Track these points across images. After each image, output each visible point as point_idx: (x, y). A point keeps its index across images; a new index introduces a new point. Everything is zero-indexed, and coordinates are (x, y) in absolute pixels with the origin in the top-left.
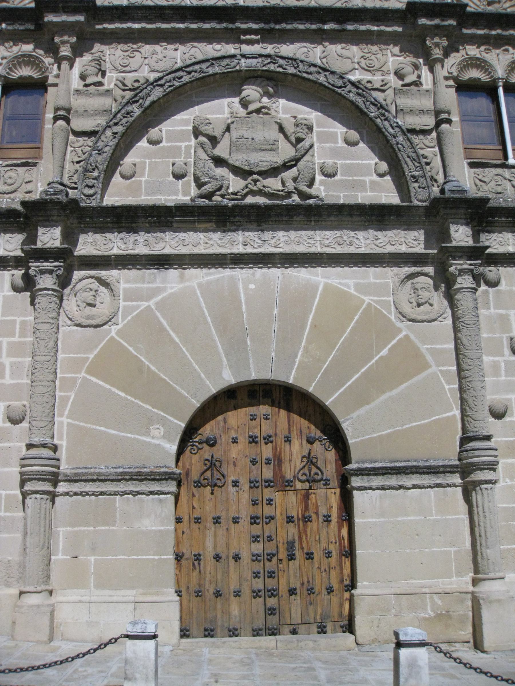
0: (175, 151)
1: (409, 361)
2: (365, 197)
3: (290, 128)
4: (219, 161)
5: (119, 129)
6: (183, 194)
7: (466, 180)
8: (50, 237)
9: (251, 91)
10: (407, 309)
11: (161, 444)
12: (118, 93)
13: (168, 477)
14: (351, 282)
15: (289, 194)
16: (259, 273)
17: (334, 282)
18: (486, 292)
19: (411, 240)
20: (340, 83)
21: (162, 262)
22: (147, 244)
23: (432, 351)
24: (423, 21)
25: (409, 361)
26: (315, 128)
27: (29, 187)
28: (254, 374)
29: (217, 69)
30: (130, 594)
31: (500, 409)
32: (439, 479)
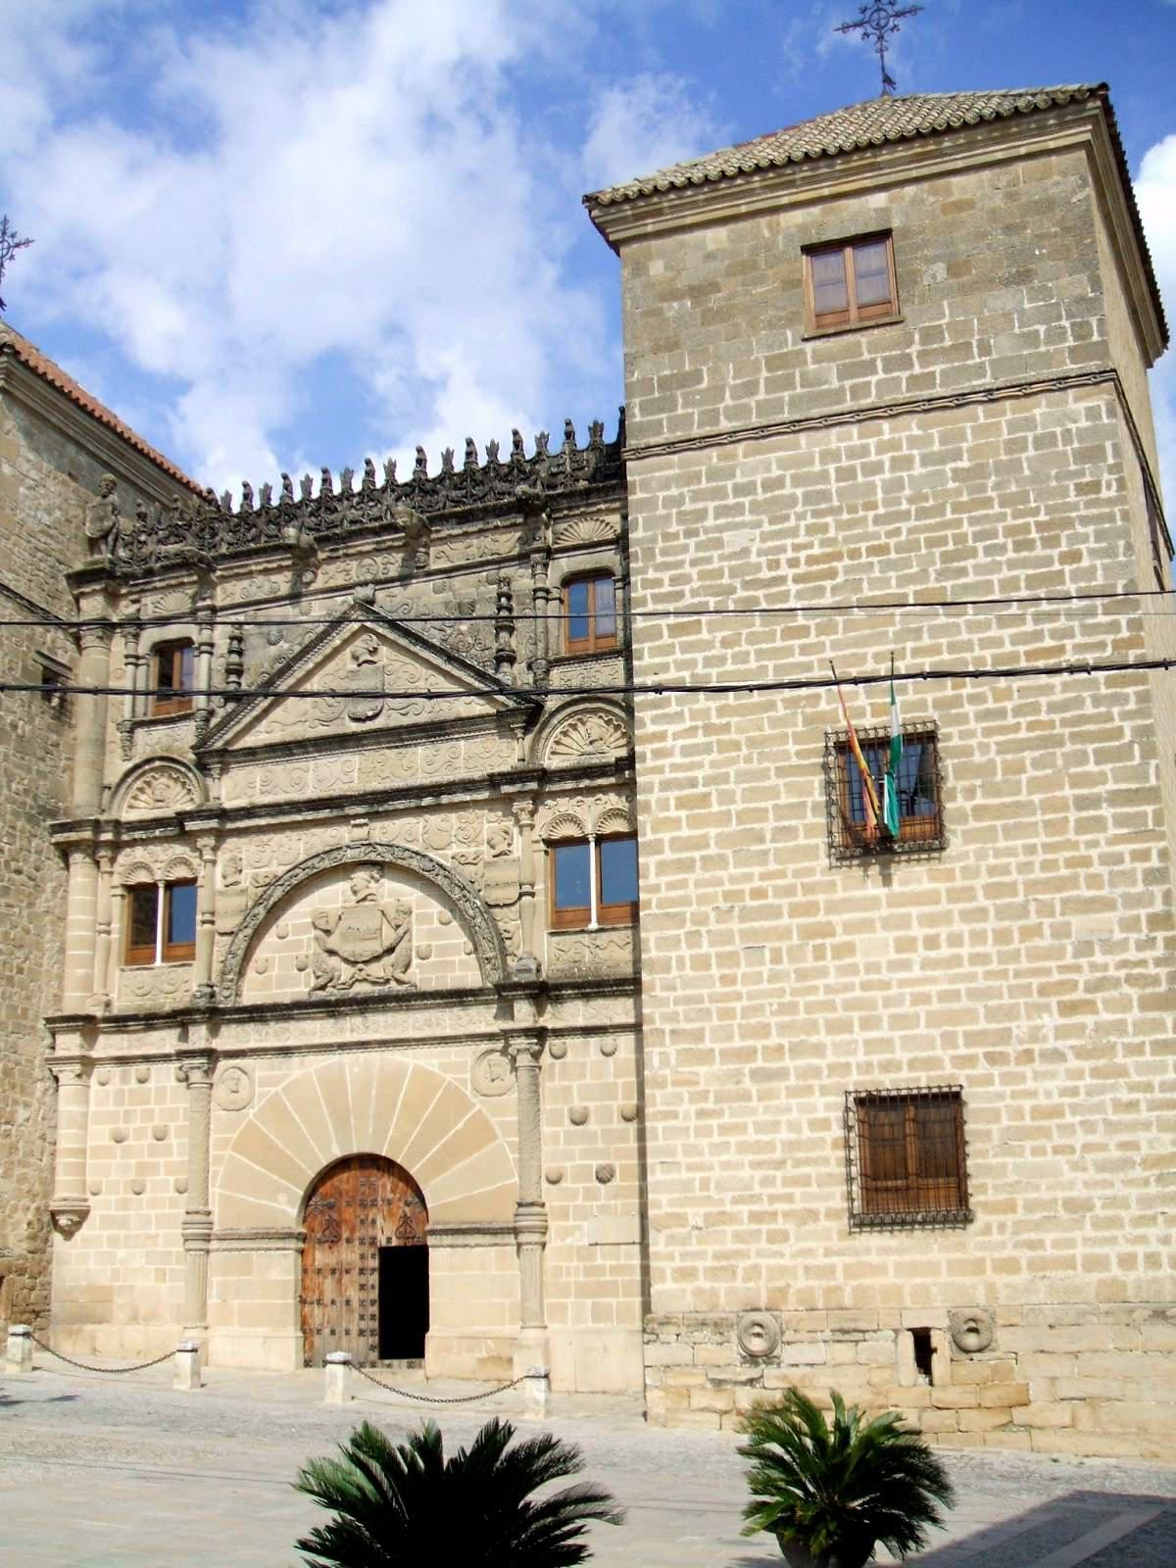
0: (299, 944)
1: (480, 1132)
2: (451, 981)
3: (391, 914)
4: (331, 953)
5: (249, 931)
6: (300, 988)
7: (542, 950)
8: (199, 1036)
9: (361, 876)
10: (485, 1085)
11: (287, 1210)
12: (252, 891)
13: (289, 1236)
14: (435, 1061)
15: (387, 981)
16: (361, 1056)
17: (422, 1063)
18: (552, 1065)
19: (482, 1018)
20: (429, 866)
21: (285, 1051)
22: (276, 1035)
23: (502, 1124)
24: (506, 789)
25: (480, 1132)
26: (415, 911)
27: (185, 987)
28: (355, 1149)
29: (326, 864)
30: (263, 1330)
31: (553, 1177)
32: (498, 1239)
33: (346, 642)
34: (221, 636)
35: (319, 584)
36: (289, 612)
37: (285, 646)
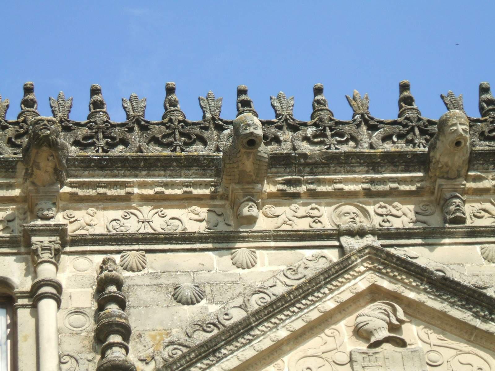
33: (343, 309)
34: (77, 274)
35: (263, 224)
36: (213, 264)
37: (213, 308)
